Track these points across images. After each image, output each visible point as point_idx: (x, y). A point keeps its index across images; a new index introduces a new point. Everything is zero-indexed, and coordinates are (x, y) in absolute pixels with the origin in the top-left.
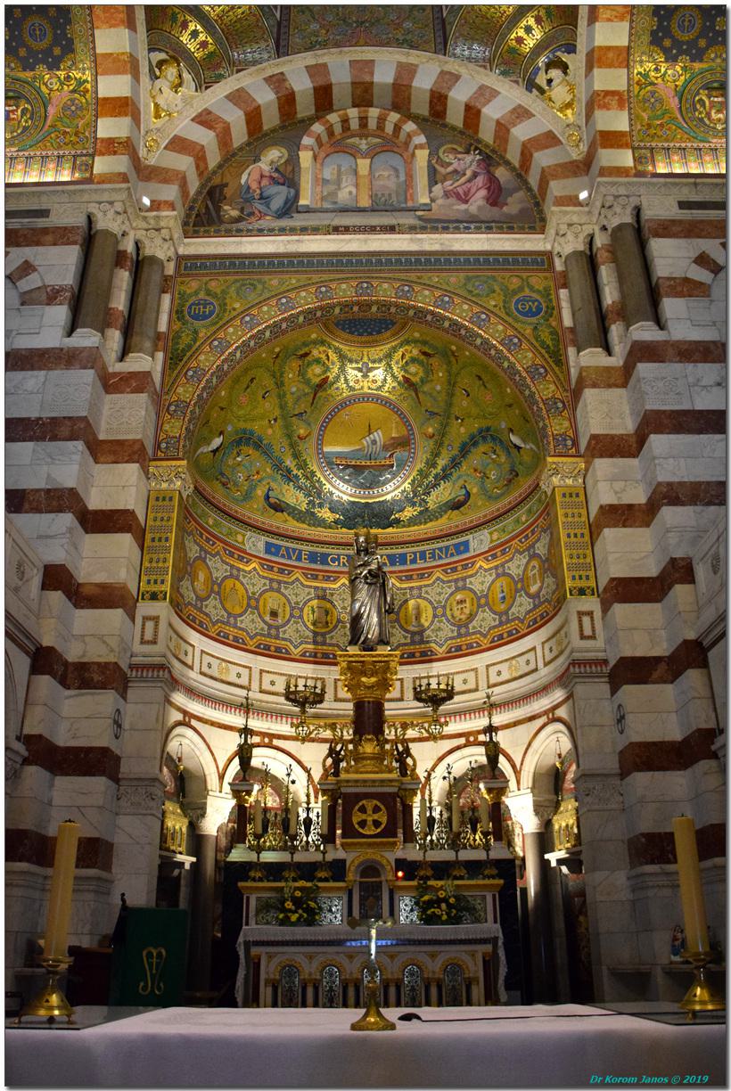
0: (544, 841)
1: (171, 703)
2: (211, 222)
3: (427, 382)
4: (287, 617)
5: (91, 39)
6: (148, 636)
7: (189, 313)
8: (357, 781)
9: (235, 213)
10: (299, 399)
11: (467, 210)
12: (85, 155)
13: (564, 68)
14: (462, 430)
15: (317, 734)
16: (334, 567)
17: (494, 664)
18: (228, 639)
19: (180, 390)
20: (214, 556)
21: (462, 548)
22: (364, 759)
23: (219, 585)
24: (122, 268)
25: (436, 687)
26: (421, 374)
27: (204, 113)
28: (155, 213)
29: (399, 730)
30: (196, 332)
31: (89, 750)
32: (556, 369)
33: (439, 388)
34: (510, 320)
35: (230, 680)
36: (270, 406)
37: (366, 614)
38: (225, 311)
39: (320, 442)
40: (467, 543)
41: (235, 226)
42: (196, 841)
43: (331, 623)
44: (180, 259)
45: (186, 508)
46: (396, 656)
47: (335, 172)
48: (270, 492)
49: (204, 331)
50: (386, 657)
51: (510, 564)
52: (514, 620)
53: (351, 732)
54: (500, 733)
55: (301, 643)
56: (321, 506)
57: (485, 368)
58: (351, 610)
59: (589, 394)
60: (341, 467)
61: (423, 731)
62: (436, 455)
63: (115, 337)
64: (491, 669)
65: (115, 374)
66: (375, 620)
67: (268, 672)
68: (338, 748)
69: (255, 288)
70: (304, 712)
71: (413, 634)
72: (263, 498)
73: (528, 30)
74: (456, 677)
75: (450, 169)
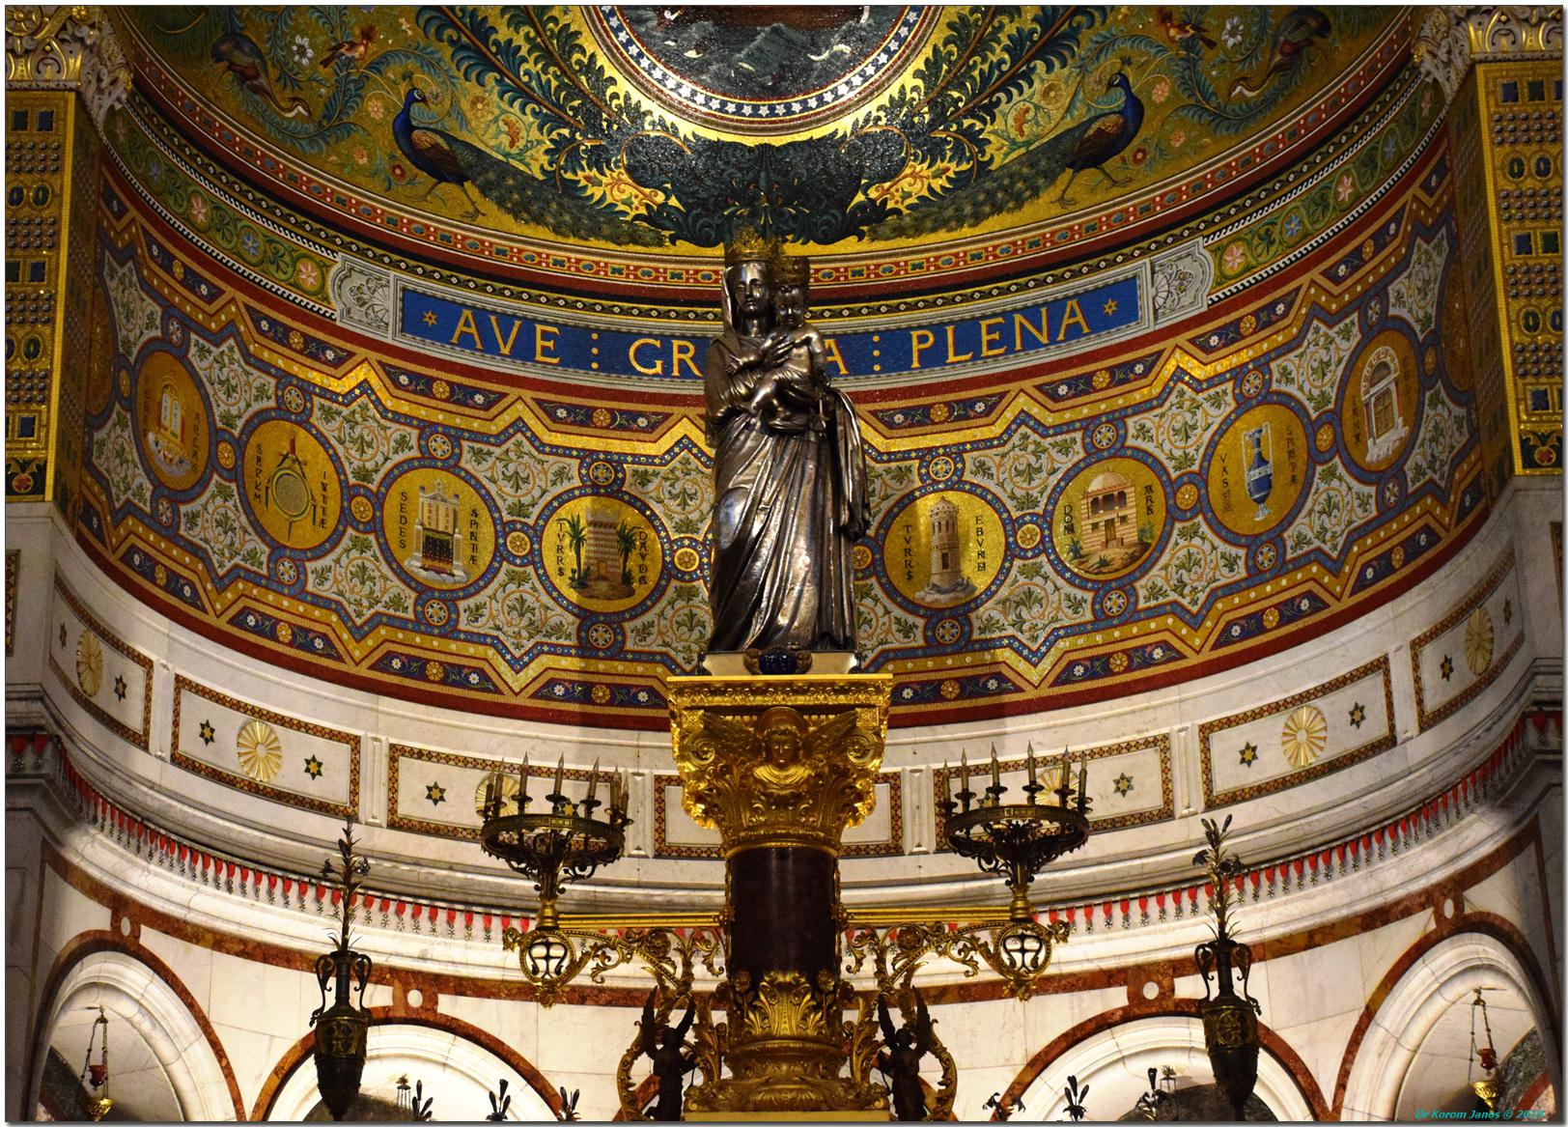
1: (67, 871)
4: (485, 557)
15: (598, 969)
16: (649, 379)
17: (1229, 722)
18: (274, 638)
21: (1110, 307)
23: (240, 446)
25: (1022, 798)
29: (889, 957)
37: (769, 541)
40: (1126, 294)
43: (643, 580)
45: (105, 158)
46: (879, 691)
48: (416, 109)
50: (843, 691)
51: (1290, 361)
52: (1300, 563)
53: (719, 961)
54: (1256, 969)
55: (535, 653)
56: (599, 159)
58: (716, 528)
60: (667, 15)
61: (978, 957)
64: (1217, 739)
66: (801, 560)
67: (420, 754)
68: (675, 1019)
70: (550, 891)
71: (933, 616)
72: (389, 130)
74: (1094, 768)
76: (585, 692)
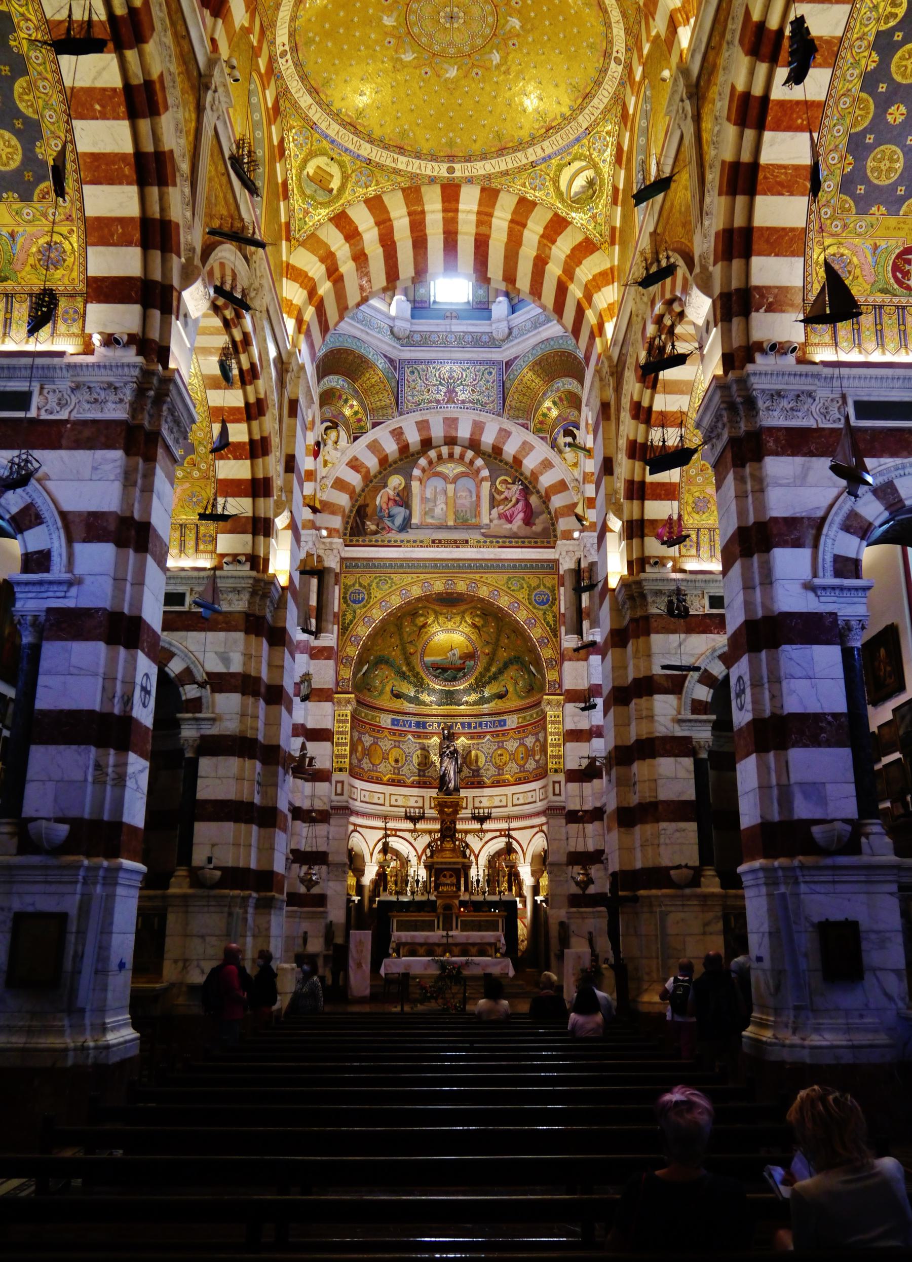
0: (536, 890)
2: (359, 535)
6: (339, 791)
9: (373, 527)
13: (574, 437)
16: (430, 729)
19: (348, 649)
28: (329, 540)
30: (355, 612)
36: (395, 640)
39: (423, 654)
40: (505, 721)
41: (374, 538)
42: (360, 888)
44: (343, 560)
59: (567, 664)
62: (490, 664)
65: (314, 648)
71: (474, 771)
73: (555, 403)
75: (503, 496)
76: (419, 782)
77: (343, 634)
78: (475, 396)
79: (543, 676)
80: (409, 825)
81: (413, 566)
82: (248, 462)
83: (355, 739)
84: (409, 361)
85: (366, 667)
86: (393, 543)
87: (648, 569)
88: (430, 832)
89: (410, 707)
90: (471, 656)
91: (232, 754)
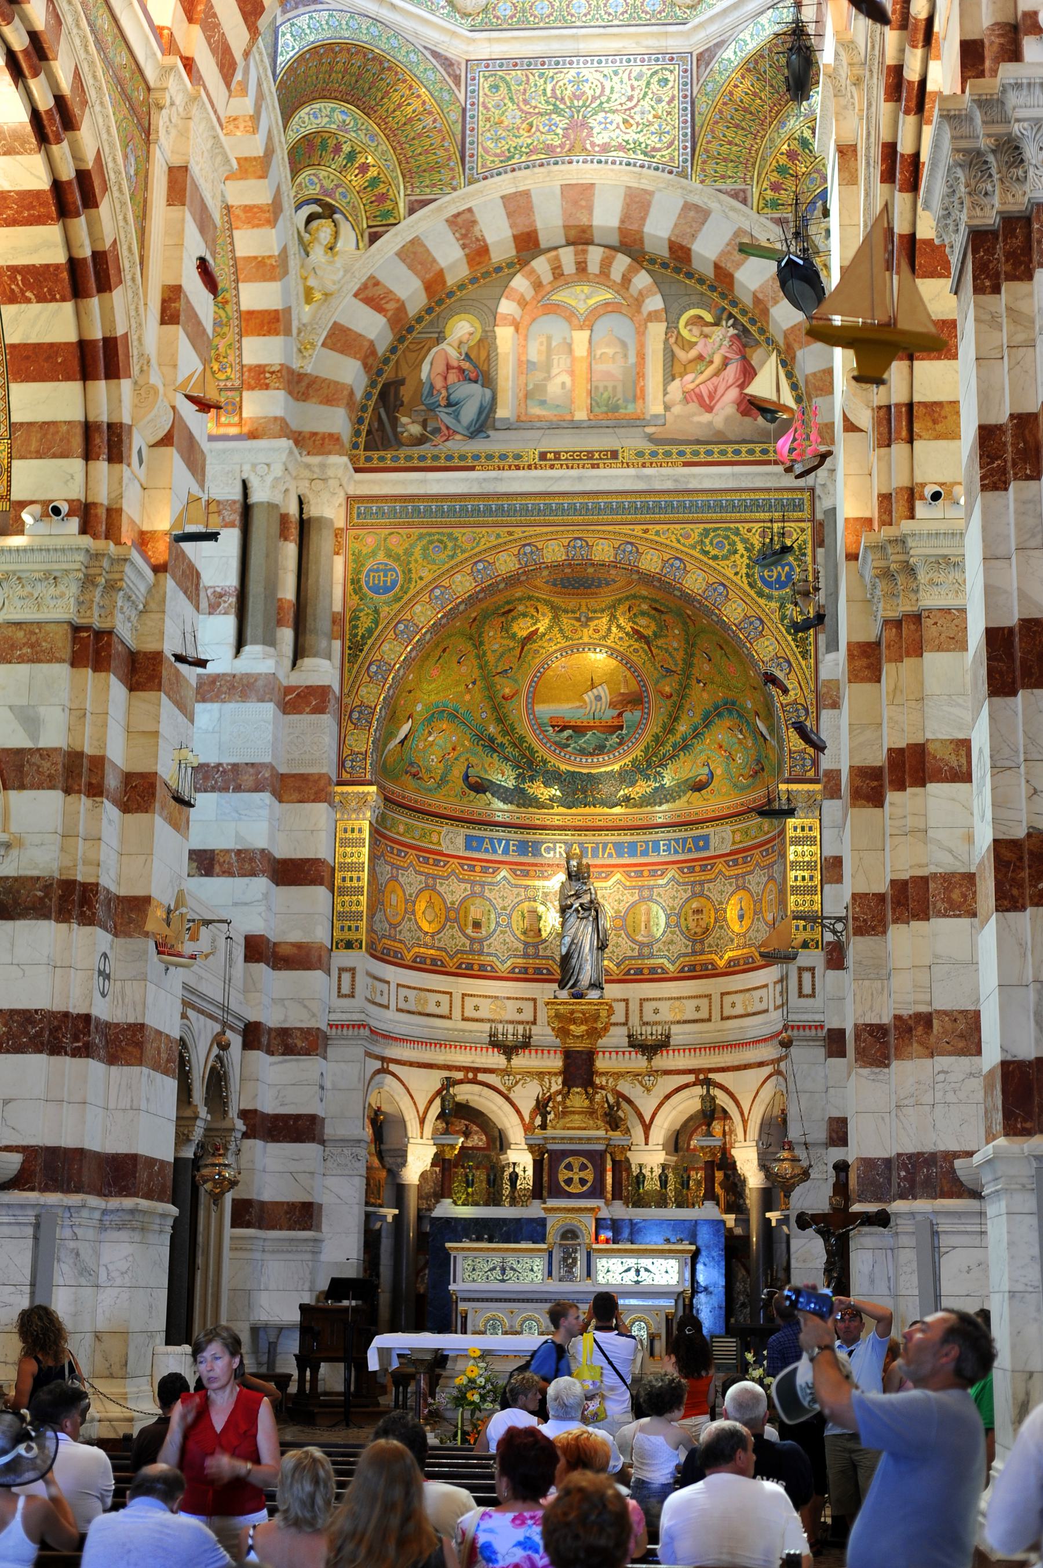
2: (386, 445)
3: (661, 636)
4: (493, 926)
5: (229, 240)
6: (346, 989)
7: (367, 583)
8: (563, 1138)
9: (415, 429)
10: (502, 655)
11: (711, 423)
12: (231, 390)
14: (705, 695)
19: (363, 691)
20: (406, 869)
21: (701, 843)
22: (574, 1113)
24: (286, 539)
26: (653, 627)
27: (370, 284)
30: (376, 611)
31: (298, 1117)
32: (803, 663)
33: (675, 645)
34: (752, 593)
35: (428, 1011)
38: (410, 580)
39: (533, 698)
40: (706, 838)
41: (416, 451)
44: (351, 500)
47: (544, 348)
49: (387, 609)
56: (532, 779)
57: (726, 642)
62: (675, 719)
63: (287, 634)
65: (288, 690)
69: (445, 548)
70: (509, 1060)
71: (642, 945)
75: (693, 353)
77: (353, 658)
78: (631, 136)
79: (780, 741)
80: (497, 1060)
81: (500, 509)
82: (68, 307)
83: (382, 880)
84: (488, 62)
85: (405, 729)
86: (456, 462)
87: (921, 509)
88: (540, 1075)
89: (500, 809)
90: (634, 700)
91: (47, 917)
